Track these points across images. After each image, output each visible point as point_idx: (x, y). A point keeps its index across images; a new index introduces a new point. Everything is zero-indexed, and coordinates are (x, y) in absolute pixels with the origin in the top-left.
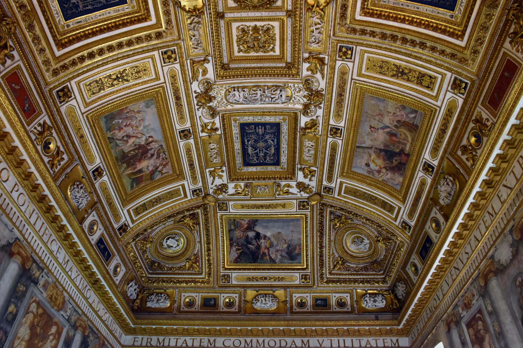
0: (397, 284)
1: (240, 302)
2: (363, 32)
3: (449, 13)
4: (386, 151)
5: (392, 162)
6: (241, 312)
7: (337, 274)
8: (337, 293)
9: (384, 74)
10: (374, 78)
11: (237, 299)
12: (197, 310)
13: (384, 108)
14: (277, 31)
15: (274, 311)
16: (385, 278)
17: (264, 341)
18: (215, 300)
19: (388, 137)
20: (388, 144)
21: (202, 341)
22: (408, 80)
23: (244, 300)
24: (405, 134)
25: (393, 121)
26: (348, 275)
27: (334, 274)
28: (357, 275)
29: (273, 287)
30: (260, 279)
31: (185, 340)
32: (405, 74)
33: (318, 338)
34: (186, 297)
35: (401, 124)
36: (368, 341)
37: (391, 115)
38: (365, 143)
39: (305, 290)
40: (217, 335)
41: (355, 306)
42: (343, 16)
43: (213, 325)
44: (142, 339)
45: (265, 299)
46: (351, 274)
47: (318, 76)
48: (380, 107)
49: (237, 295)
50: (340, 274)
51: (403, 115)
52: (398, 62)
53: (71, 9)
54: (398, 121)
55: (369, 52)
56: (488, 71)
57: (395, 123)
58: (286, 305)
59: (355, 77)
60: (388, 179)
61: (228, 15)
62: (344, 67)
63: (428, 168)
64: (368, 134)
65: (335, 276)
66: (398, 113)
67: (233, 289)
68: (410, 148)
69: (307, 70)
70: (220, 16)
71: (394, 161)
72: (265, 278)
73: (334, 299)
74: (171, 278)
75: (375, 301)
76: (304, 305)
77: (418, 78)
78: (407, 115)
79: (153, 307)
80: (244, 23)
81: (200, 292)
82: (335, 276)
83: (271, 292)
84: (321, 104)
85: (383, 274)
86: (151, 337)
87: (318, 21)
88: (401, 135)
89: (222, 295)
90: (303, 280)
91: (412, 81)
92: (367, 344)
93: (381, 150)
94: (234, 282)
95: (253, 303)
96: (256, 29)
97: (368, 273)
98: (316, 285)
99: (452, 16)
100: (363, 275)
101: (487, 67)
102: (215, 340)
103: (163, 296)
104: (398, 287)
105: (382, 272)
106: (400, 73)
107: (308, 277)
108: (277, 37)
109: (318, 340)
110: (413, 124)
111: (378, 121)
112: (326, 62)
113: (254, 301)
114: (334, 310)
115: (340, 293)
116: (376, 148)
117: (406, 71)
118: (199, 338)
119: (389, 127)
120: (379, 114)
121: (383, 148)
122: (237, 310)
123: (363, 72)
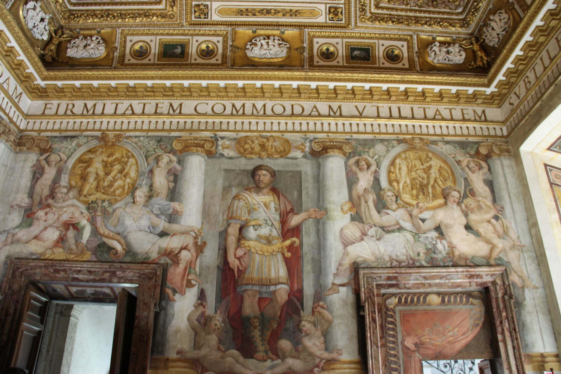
0: (491, 17)
1: (225, 48)
6: (226, 63)
7: (388, 9)
8: (386, 39)
11: (220, 46)
12: (152, 62)
15: (282, 63)
16: (464, 19)
17: (264, 106)
18: (184, 46)
21: (159, 106)
23: (231, 46)
26: (407, 10)
27: (382, 8)
28: (420, 11)
29: (281, 25)
30: (259, 12)
31: (131, 105)
33: (356, 104)
34: (135, 42)
36: (437, 110)
39: (333, 32)
40: (185, 96)
41: (416, 59)
43: (178, 78)
44: (59, 105)
45: (268, 43)
46: (411, 10)
49: (220, 39)
50: (392, 9)
58: (301, 54)
65: (385, 12)
67: (213, 28)
72: (268, 12)
73: (380, 49)
74: (109, 10)
75: (448, 52)
76: (331, 56)
79: (78, 57)
81: (157, 34)
82: (385, 12)
83: (277, 32)
85: (461, 13)
86: (74, 102)
89: (195, 38)
90: (331, 15)
92: (436, 114)
94: (216, 17)
95: (246, 49)
97: (437, 10)
98: (353, 24)
100: (429, 12)
102: (181, 105)
103: (94, 38)
104: (493, 24)
105: (460, 10)
107: (340, 10)
109: (356, 107)
113: (248, 46)
114: (381, 65)
115: (391, 39)
118: (153, 102)
122: (220, 62)
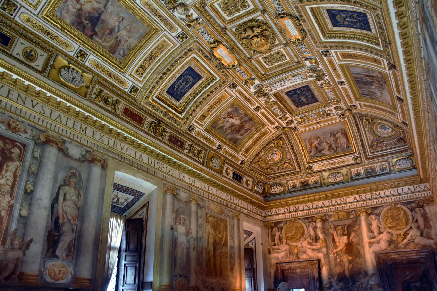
2: (185, 54)
3: (166, 90)
4: (98, 18)
5: (86, 19)
9: (155, 48)
10: (157, 42)
13: (134, 36)
14: (225, 15)
19: (110, 27)
20: (104, 24)
22: (145, 60)
24: (109, 42)
25: (122, 38)
32: (149, 60)
35: (118, 42)
37: (127, 39)
38: (112, 5)
42: (200, 50)
47: (184, 17)
48: (135, 34)
51: (123, 46)
52: (157, 59)
53: (362, 17)
54: (120, 41)
55: (172, 48)
56: (140, 109)
57: (120, 38)
59: (165, 32)
60: (68, 5)
61: (260, 13)
62: (175, 31)
63: (82, 54)
64: (118, 13)
66: (126, 44)
68: (97, 41)
69: (192, 14)
70: (264, 11)
71: (87, 22)
77: (144, 66)
78: (123, 49)
80: (247, 10)
84: (165, 3)
87: (210, 41)
88: (109, 38)
91: (144, 62)
93: (100, 15)
96: (238, 10)
99: (164, 91)
101: (142, 109)
106: (151, 57)
108: (222, 13)
110: (115, 51)
111: (126, 27)
112: (187, 27)
116: (103, 12)
117: (151, 61)
119: (118, 32)
120: (130, 29)
121: (101, 17)
123: (164, 38)
